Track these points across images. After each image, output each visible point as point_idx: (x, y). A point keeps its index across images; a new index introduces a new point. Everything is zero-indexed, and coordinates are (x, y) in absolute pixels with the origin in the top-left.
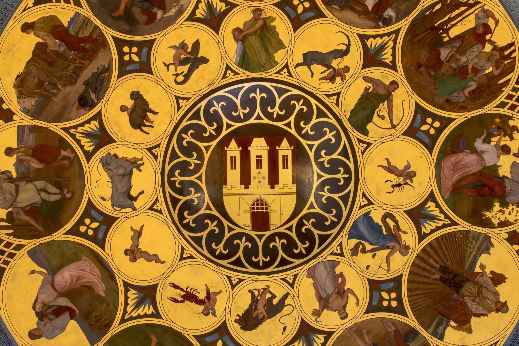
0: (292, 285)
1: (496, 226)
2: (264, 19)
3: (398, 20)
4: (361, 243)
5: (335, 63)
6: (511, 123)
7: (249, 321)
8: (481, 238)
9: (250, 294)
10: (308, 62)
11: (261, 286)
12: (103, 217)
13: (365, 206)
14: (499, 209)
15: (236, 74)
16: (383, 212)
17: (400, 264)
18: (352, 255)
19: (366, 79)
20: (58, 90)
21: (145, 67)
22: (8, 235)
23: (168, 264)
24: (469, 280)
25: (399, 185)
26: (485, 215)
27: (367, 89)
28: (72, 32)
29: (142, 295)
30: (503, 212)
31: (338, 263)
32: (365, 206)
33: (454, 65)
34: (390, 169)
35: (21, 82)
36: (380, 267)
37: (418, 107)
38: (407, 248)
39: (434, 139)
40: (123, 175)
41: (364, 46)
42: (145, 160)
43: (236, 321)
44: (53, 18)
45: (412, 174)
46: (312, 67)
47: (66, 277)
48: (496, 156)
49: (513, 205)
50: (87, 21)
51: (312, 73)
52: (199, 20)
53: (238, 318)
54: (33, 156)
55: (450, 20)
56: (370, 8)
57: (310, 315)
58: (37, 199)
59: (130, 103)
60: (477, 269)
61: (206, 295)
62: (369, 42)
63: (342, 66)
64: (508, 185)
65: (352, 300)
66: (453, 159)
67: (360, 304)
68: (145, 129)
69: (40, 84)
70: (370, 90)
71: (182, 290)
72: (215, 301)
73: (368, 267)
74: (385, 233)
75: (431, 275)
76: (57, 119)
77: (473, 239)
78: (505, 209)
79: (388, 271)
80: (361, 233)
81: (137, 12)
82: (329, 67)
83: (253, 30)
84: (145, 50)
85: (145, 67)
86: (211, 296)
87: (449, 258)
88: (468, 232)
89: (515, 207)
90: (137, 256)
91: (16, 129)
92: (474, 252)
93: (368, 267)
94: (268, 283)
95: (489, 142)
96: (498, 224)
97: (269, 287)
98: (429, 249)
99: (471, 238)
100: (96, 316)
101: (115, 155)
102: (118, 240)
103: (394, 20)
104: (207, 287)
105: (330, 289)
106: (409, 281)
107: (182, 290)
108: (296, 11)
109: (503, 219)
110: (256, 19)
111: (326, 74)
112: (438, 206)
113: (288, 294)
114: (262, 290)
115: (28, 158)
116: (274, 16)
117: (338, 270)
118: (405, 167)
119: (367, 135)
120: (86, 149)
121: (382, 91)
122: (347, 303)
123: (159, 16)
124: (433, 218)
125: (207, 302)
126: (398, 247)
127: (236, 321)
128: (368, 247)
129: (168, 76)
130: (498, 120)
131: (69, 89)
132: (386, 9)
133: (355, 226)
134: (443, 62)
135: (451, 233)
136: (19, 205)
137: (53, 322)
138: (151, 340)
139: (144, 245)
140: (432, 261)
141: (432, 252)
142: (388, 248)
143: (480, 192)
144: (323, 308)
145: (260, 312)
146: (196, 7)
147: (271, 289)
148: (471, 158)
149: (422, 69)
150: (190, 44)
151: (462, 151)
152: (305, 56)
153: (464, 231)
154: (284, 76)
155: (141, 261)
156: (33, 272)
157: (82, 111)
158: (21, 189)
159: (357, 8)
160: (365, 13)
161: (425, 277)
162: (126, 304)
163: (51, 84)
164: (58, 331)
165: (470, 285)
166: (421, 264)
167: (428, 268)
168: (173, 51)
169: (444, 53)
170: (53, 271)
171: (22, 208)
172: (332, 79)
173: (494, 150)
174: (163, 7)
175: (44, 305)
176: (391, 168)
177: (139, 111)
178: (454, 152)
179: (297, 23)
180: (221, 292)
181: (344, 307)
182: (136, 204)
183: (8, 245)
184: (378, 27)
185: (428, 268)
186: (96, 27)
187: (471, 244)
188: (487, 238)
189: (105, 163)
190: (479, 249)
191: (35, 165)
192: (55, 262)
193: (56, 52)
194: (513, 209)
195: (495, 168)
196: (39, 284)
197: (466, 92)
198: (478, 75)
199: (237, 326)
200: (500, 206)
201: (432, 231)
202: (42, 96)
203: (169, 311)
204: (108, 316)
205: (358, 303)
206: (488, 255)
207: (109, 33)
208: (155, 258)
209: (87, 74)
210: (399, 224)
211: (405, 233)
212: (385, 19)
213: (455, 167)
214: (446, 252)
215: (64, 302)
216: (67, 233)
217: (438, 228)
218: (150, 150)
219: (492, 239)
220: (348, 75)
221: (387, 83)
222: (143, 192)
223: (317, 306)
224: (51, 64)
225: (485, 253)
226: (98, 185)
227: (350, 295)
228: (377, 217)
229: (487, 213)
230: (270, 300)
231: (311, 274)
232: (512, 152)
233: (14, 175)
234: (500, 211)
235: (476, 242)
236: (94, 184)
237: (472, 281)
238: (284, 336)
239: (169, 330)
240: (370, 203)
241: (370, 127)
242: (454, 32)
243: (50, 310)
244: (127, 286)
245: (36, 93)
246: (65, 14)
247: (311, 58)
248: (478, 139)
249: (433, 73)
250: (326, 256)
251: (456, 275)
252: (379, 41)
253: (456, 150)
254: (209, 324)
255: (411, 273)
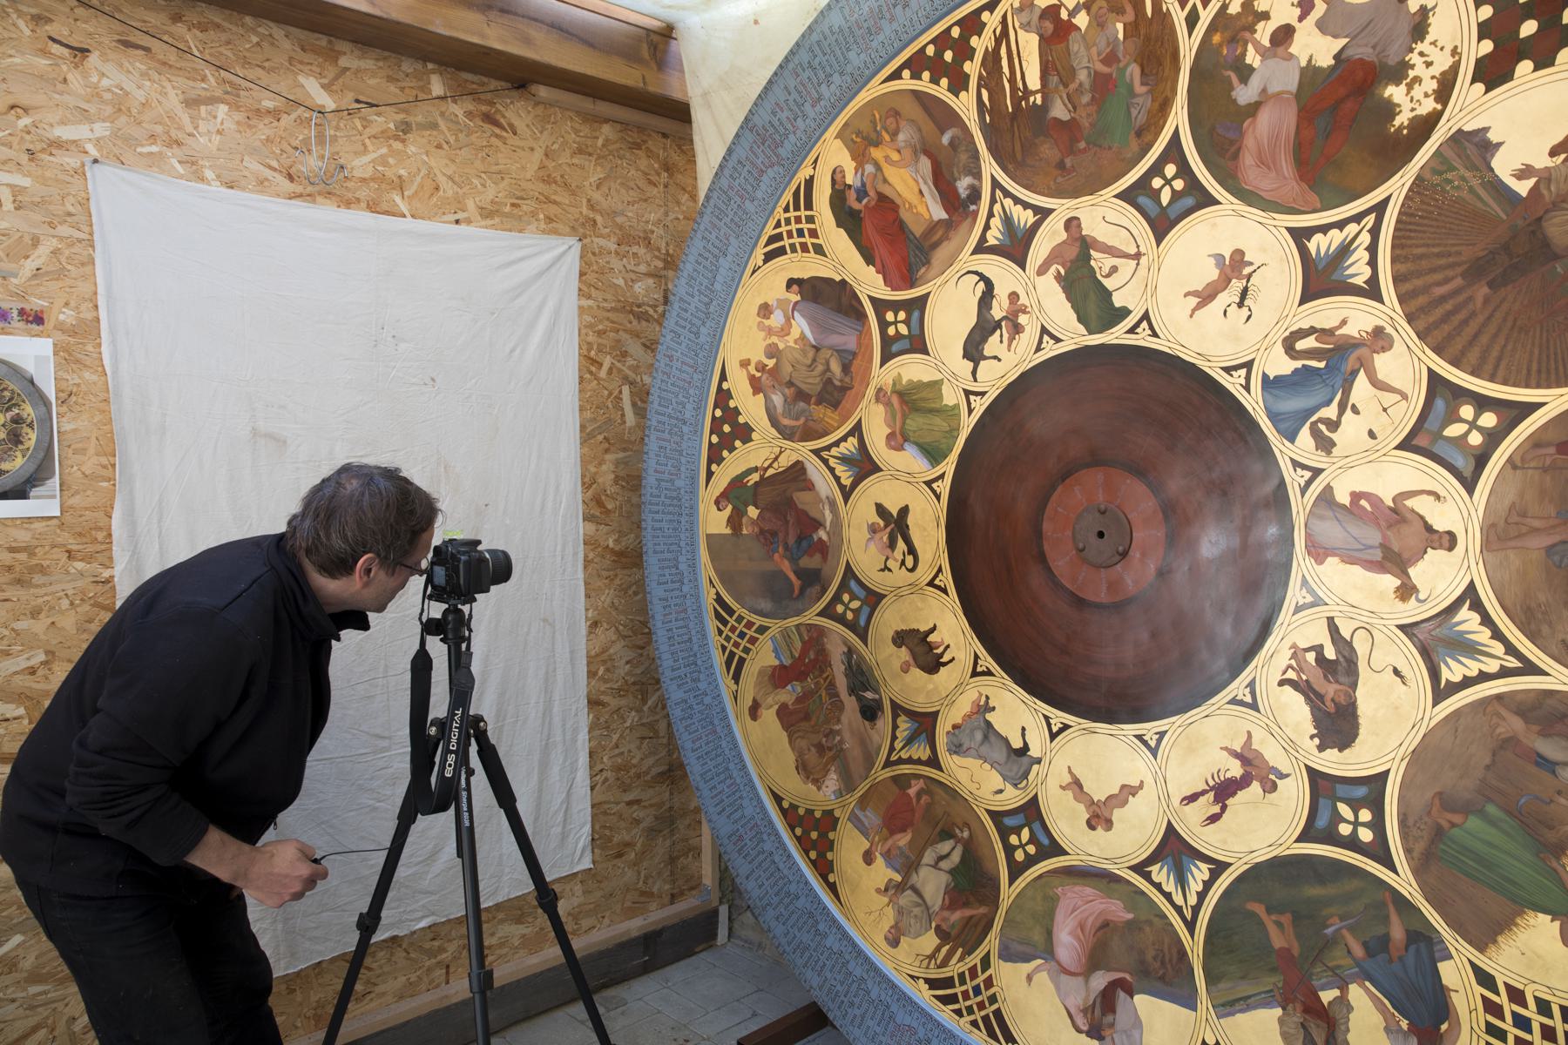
0: (1318, 602)
1: (1439, 107)
2: (893, 392)
3: (978, 175)
4: (1314, 424)
5: (997, 312)
6: (1234, 8)
7: (1337, 724)
8: (1449, 153)
9: (1287, 689)
10: (976, 356)
11: (1284, 658)
12: (1022, 815)
13: (1248, 378)
14: (1403, 87)
15: (942, 476)
16: (1279, 349)
17: (1406, 364)
18: (1329, 453)
19: (1041, 271)
20: (838, 732)
21: (874, 599)
22: (961, 959)
23: (1149, 780)
24: (1540, 219)
25: (1244, 293)
26: (1401, 127)
27: (1058, 277)
28: (787, 662)
29: (1170, 859)
30: (1417, 80)
31: (1328, 489)
32: (1248, 378)
33: (1086, 99)
34: (1206, 296)
35: (803, 768)
36: (1385, 410)
37: (1126, 196)
38: (1378, 332)
39: (1194, 184)
40: (986, 737)
41: (993, 250)
42: (985, 691)
43: (1321, 748)
44: (761, 672)
45: (1237, 258)
46: (986, 353)
47: (1067, 942)
48: (1285, 63)
49: (1411, 50)
50: (785, 634)
51: (995, 358)
52: (855, 485)
53: (1317, 741)
54: (892, 833)
55: (1012, 80)
56: (944, 216)
57: (1400, 605)
58: (944, 878)
59: (904, 654)
60: (1523, 188)
61: (1238, 763)
62: (992, 241)
63: (1006, 304)
64: (1360, 50)
65: (1420, 505)
66: (1248, 159)
67: (1442, 493)
68: (944, 660)
69: (821, 749)
70: (1063, 272)
71: (1203, 793)
72: (1259, 755)
73: (1372, 435)
74: (1322, 365)
75: (1471, 306)
76: (869, 761)
77: (1440, 173)
78: (1411, 73)
79: (1405, 397)
80: (1297, 412)
81: (807, 562)
82: (998, 325)
83: (899, 416)
84: (853, 584)
85: (874, 599)
86: (1246, 754)
87: (1454, 249)
88: (1419, 180)
89: (1419, 47)
90: (1106, 814)
91: (849, 825)
92: (1475, 183)
93: (1372, 435)
94: (1287, 643)
95: (1251, 69)
96: (1436, 100)
97: (1294, 646)
98: (1408, 286)
99: (1436, 179)
100: (1155, 958)
101: (955, 727)
102: (1066, 820)
103: (976, 182)
104: (1226, 749)
105: (1373, 536)
106: (1455, 363)
107: (1203, 793)
108: (903, 337)
109: (1434, 85)
110: (888, 404)
111: (1006, 336)
112: (1324, 229)
113: (1331, 620)
114: (1293, 662)
115: (890, 842)
116: (894, 374)
117: (1343, 498)
118: (1217, 265)
119: (1129, 312)
120: (924, 758)
121: (1072, 252)
122: (1422, 518)
123: (824, 537)
124: (1345, 250)
125: (1254, 771)
126: (1363, 351)
127: (1321, 748)
128: (1331, 412)
129: (900, 576)
130: (1217, 38)
131: (844, 718)
132: (955, 190)
133: (1273, 417)
134: (1073, 119)
135: (1398, 221)
136: (937, 908)
137: (1118, 1026)
138: (1254, 915)
139: (1099, 791)
140: (1439, 291)
141: (1418, 282)
142: (1354, 373)
143: (1345, 124)
144: (1402, 572)
145: (1331, 694)
146: (837, 479)
147: (1303, 645)
148: (1264, 119)
149: (1068, 162)
150: (874, 518)
151: (1242, 134)
152: (966, 355)
153: (1410, 190)
154: (980, 405)
155: (1117, 815)
156: (1029, 978)
157: (880, 723)
158: (918, 886)
159: (936, 238)
160: (948, 226)
161: (1465, 322)
162: (1168, 896)
163: (826, 736)
164: (1136, 1033)
165: (1555, 221)
166: (1431, 320)
167: (1449, 306)
168: (873, 547)
169: (1059, 111)
170: (1048, 952)
171: (942, 908)
172: (1017, 329)
173: (1272, 62)
174: (818, 524)
175: (1084, 1011)
176: (1205, 294)
177: (920, 649)
178: (1236, 156)
179: (918, 345)
180: (1249, 734)
181: (1429, 528)
182: (1034, 752)
183: (973, 972)
184: (976, 213)
185: (1449, 306)
186: (798, 627)
187: (1449, 181)
188: (1459, 137)
189: (956, 749)
190: (1473, 167)
191: (903, 840)
192: (1037, 936)
193: (798, 700)
194: (1421, 54)
195: (1310, 73)
196: (1051, 986)
197: (1140, 89)
198: (1120, 55)
199: (1332, 753)
200: (1397, 85)
201: (1373, 263)
202: (834, 759)
203: (1225, 842)
204: (1167, 940)
205: (1438, 497)
206: (1502, 149)
207: (811, 617)
208: (1126, 791)
209: (842, 683)
210: (1318, 326)
211: (1344, 322)
212: (968, 197)
213: (1265, 161)
214: (1436, 250)
215: (1100, 980)
216: (1011, 882)
217: (1373, 249)
218: (975, 674)
219: (1466, 128)
220: (1023, 300)
221: (1064, 236)
222: (1024, 729)
223: (1390, 582)
224: (807, 717)
225: (1493, 156)
226: (980, 783)
227: (1409, 503)
228: (1282, 365)
229: (1397, 122)
230: (1321, 659)
231: (1319, 552)
232: (1295, 23)
233: (898, 878)
234: (1410, 87)
235: (1454, 169)
236: (973, 787)
237: (1546, 212)
238: (1413, 684)
239: (1258, 873)
240: (1248, 365)
241: (1118, 301)
242: (1034, 82)
243: (1098, 1011)
244: (1140, 869)
245: (827, 764)
246: (764, 657)
247: (973, 350)
248: (1234, 94)
249: (1082, 145)
250: (1300, 506)
251: (1506, 248)
252: (996, 222)
253: (1233, 149)
254: (1294, 795)
255: (1438, 350)
